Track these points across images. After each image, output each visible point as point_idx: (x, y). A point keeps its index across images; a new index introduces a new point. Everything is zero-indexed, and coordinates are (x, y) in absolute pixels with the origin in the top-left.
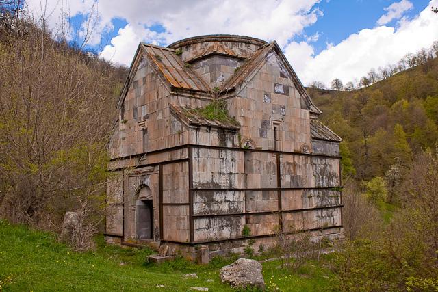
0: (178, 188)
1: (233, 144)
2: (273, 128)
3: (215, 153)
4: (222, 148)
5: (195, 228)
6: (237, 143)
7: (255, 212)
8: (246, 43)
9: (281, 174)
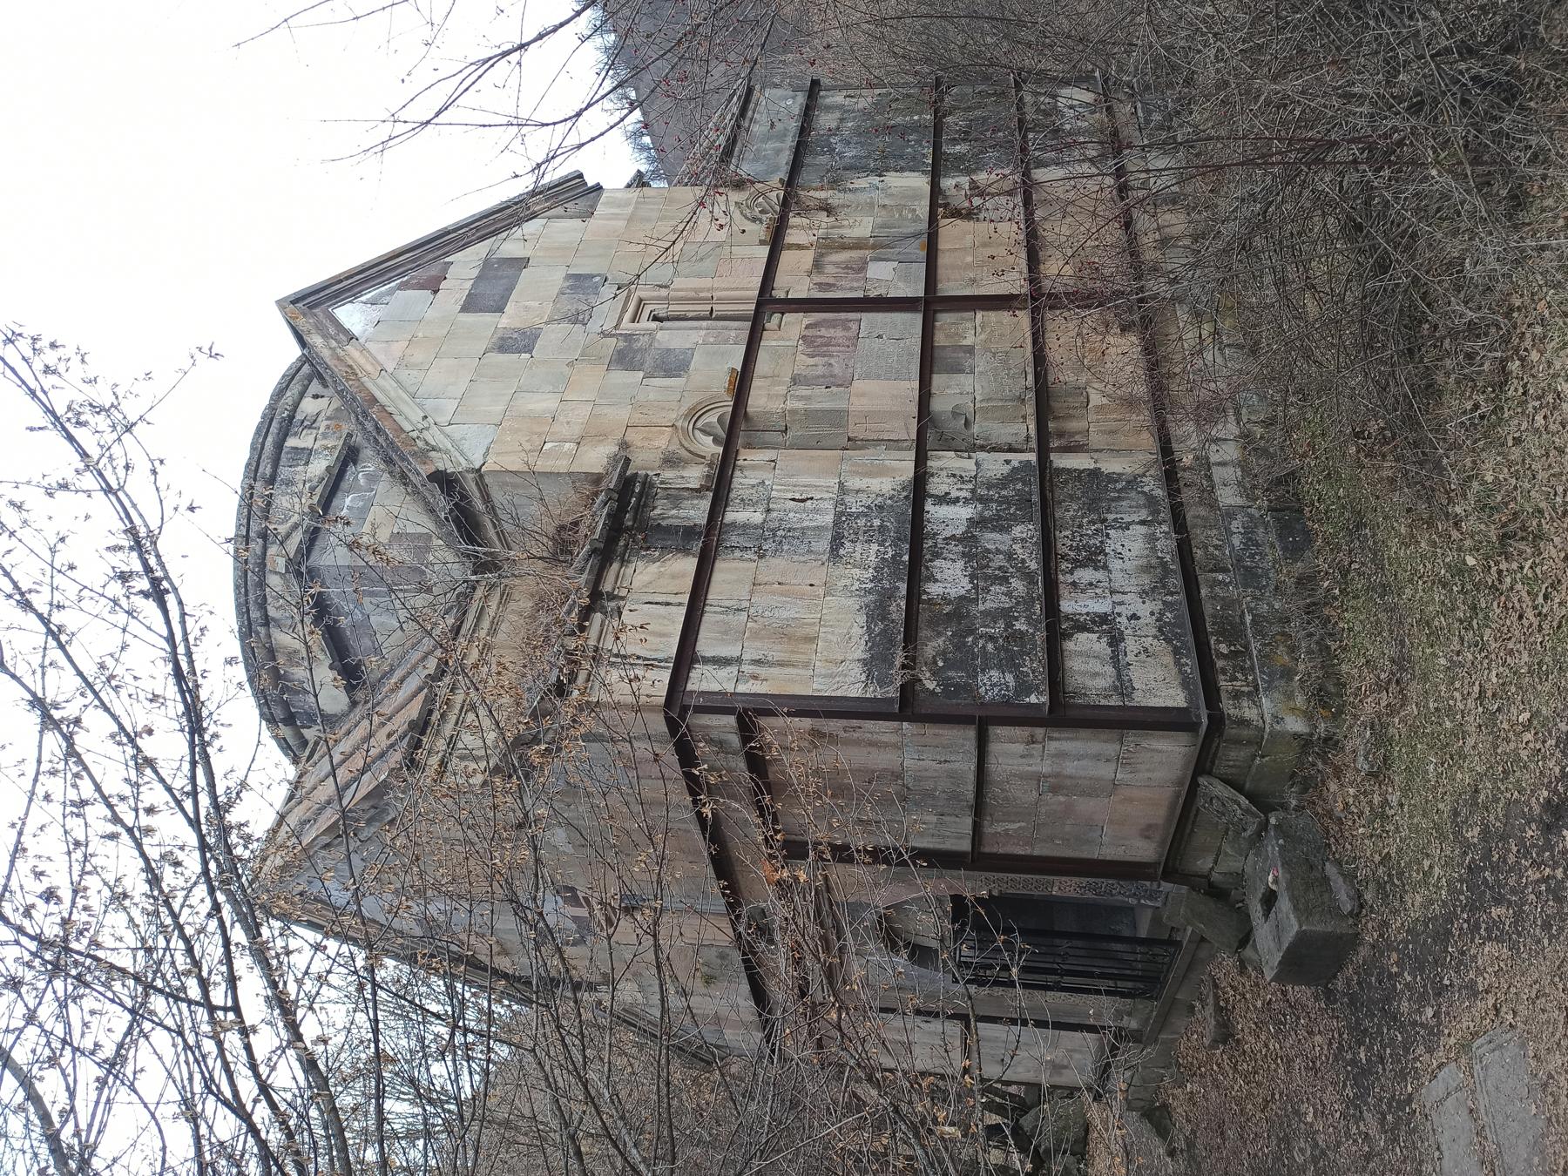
0: (897, 775)
2: (654, 325)
3: (729, 577)
4: (708, 544)
5: (1115, 701)
6: (694, 475)
7: (1030, 409)
8: (284, 434)
9: (860, 294)
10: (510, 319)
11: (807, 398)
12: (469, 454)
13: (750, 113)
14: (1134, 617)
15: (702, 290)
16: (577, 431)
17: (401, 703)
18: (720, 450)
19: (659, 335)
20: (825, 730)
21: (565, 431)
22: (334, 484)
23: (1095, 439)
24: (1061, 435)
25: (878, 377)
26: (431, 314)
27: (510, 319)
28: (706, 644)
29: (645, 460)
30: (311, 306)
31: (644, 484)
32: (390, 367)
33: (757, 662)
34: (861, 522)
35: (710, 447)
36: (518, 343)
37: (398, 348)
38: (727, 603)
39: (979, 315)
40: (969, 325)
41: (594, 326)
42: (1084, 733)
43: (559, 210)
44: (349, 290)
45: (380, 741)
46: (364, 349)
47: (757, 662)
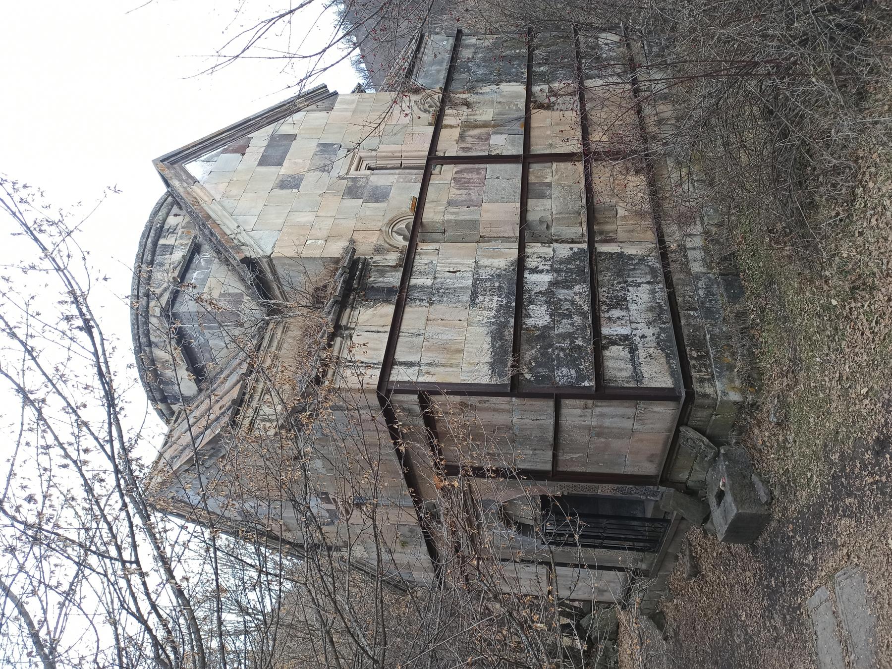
0: (509, 428)
1: (395, 268)
2: (369, 172)
3: (413, 316)
4: (401, 297)
6: (392, 258)
7: (584, 218)
8: (159, 235)
9: (486, 154)
10: (286, 169)
11: (457, 213)
12: (264, 248)
13: (422, 49)
14: (643, 336)
15: (396, 152)
16: (325, 233)
17: (227, 390)
18: (407, 243)
19: (372, 178)
20: (468, 402)
21: (319, 234)
22: (187, 265)
23: (621, 235)
24: (601, 233)
25: (497, 201)
26: (241, 167)
27: (286, 169)
28: (401, 355)
29: (364, 249)
30: (173, 162)
31: (364, 264)
32: (218, 198)
33: (430, 364)
34: (488, 284)
35: (401, 242)
36: (291, 183)
37: (222, 187)
38: (412, 331)
39: (554, 165)
40: (549, 171)
41: (334, 173)
42: (615, 402)
43: (314, 107)
44: (194, 153)
45: (216, 411)
46: (202, 188)
47: (430, 364)
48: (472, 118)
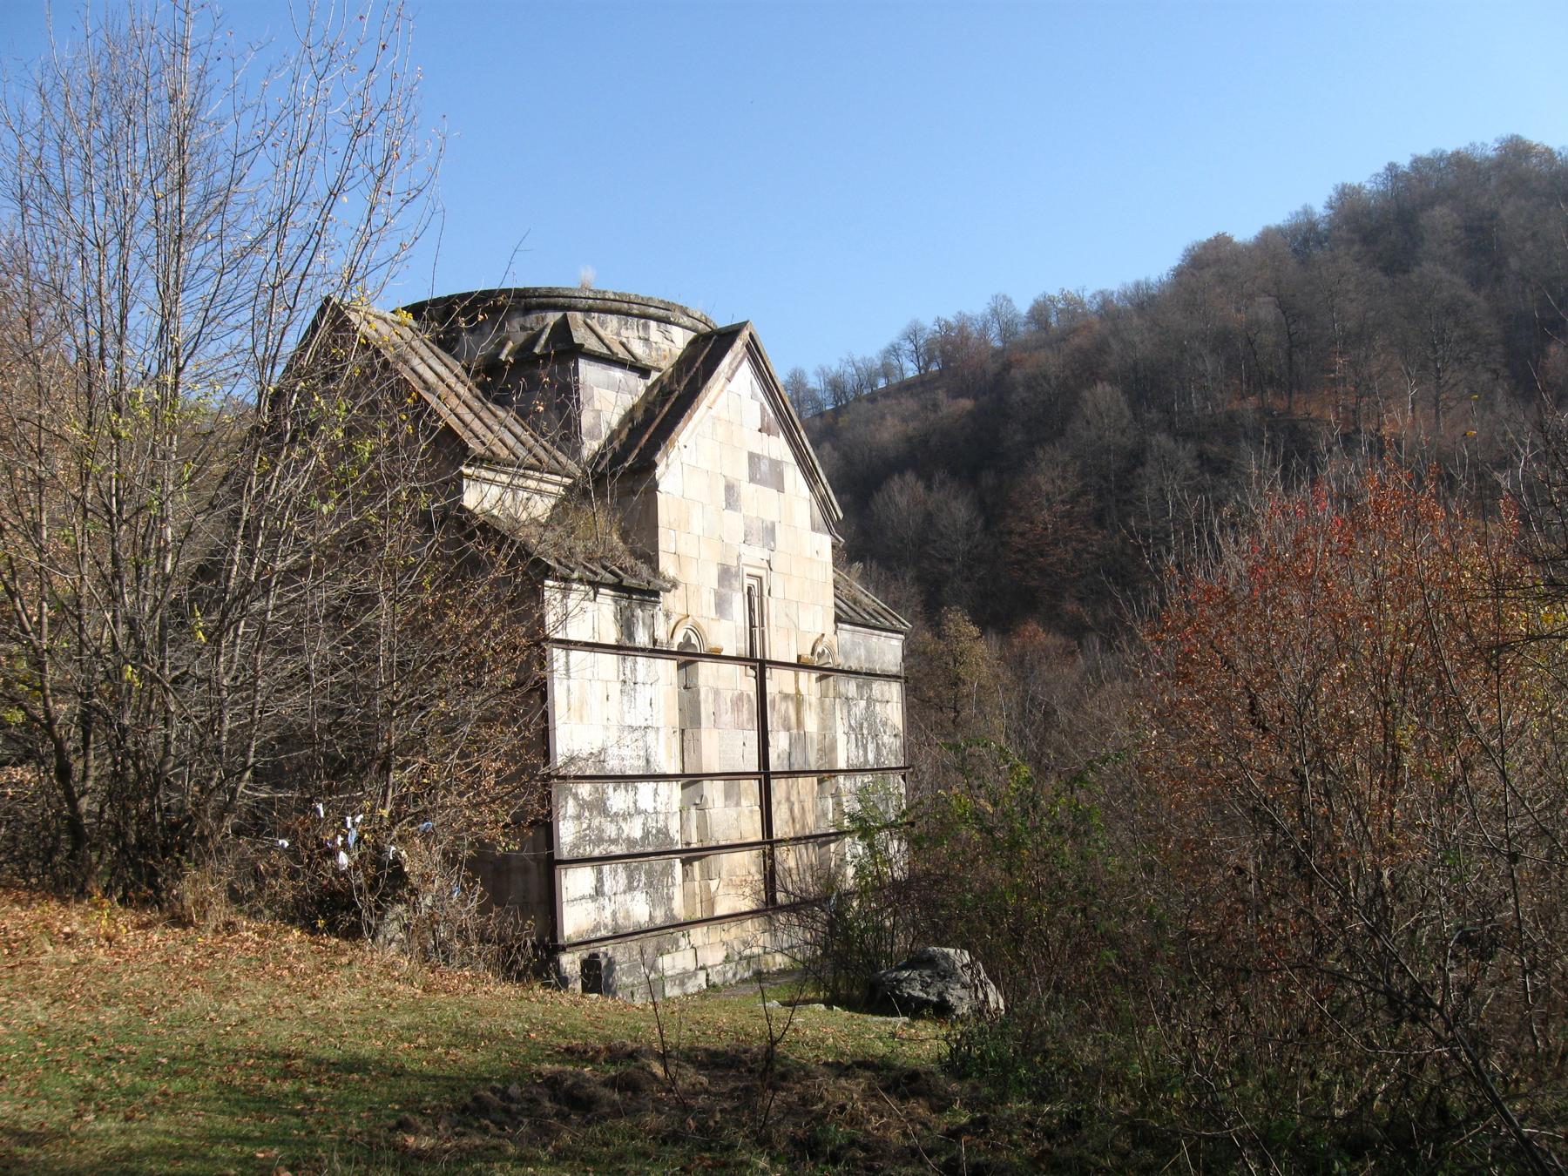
10: (747, 490)
16: (681, 551)
27: (747, 490)
28: (576, 656)
29: (667, 599)
36: (731, 494)
48: (806, 707)
